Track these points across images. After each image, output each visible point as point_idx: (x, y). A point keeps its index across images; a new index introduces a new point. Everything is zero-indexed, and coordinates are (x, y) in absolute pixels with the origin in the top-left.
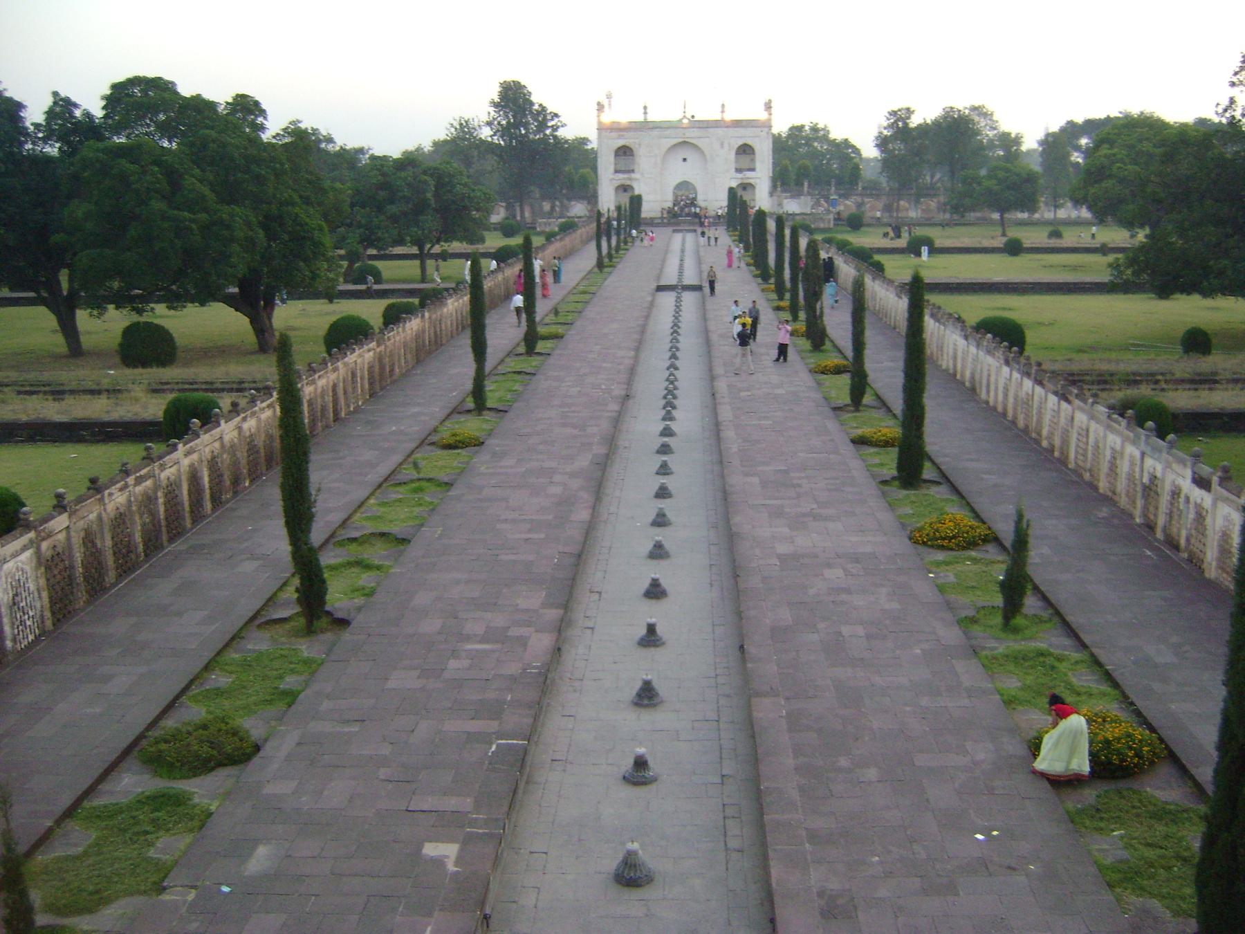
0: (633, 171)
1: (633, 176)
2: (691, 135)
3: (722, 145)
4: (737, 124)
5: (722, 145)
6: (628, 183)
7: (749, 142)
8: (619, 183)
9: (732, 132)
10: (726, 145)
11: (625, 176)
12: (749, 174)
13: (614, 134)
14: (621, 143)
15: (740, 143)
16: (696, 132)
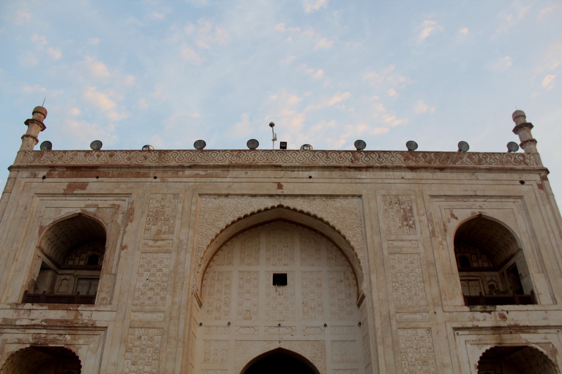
0: (89, 300)
1: (86, 313)
2: (305, 193)
3: (407, 218)
4: (441, 162)
5: (407, 218)
6: (64, 340)
7: (493, 211)
8: (28, 338)
9: (434, 182)
10: (420, 220)
11: (57, 314)
12: (516, 314)
13: (59, 184)
14: (72, 206)
15: (464, 214)
16: (321, 183)
